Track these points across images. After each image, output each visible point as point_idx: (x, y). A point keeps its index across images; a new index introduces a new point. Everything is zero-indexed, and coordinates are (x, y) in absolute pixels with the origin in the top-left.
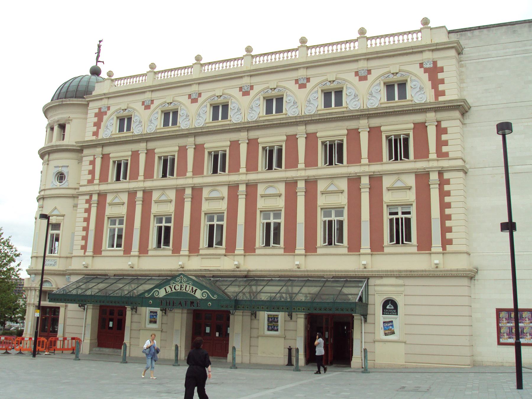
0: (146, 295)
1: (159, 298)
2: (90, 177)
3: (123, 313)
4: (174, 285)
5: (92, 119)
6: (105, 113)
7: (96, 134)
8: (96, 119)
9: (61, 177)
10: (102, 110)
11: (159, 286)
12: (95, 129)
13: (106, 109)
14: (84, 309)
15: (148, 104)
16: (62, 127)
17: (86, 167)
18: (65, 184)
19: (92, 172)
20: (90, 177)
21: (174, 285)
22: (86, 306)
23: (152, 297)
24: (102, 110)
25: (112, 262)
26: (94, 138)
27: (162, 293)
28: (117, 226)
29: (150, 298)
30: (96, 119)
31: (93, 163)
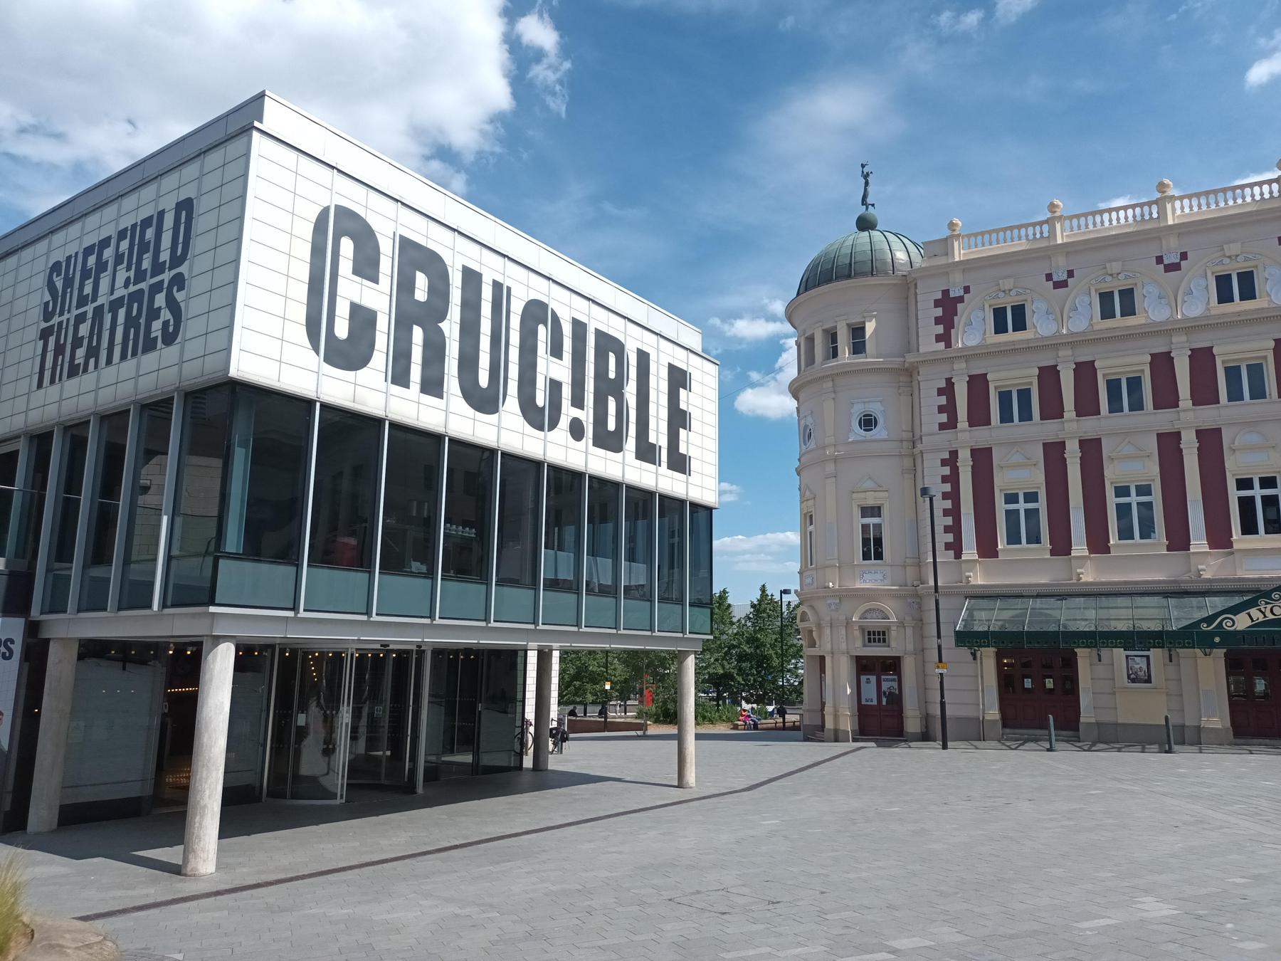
0: (1204, 626)
1: (1236, 632)
2: (944, 418)
3: (1070, 663)
4: (1269, 606)
5: (928, 312)
6: (961, 299)
7: (945, 338)
8: (939, 312)
9: (868, 422)
10: (952, 295)
11: (1235, 610)
12: (940, 329)
13: (962, 293)
14: (975, 658)
15: (1061, 279)
16: (857, 332)
17: (931, 401)
18: (879, 432)
19: (949, 409)
20: (944, 418)
21: (1269, 606)
22: (978, 654)
23: (1220, 631)
24: (952, 295)
25: (1026, 566)
26: (942, 345)
27: (1242, 622)
28: (1022, 506)
29: (1212, 634)
30: (939, 312)
31: (948, 390)
